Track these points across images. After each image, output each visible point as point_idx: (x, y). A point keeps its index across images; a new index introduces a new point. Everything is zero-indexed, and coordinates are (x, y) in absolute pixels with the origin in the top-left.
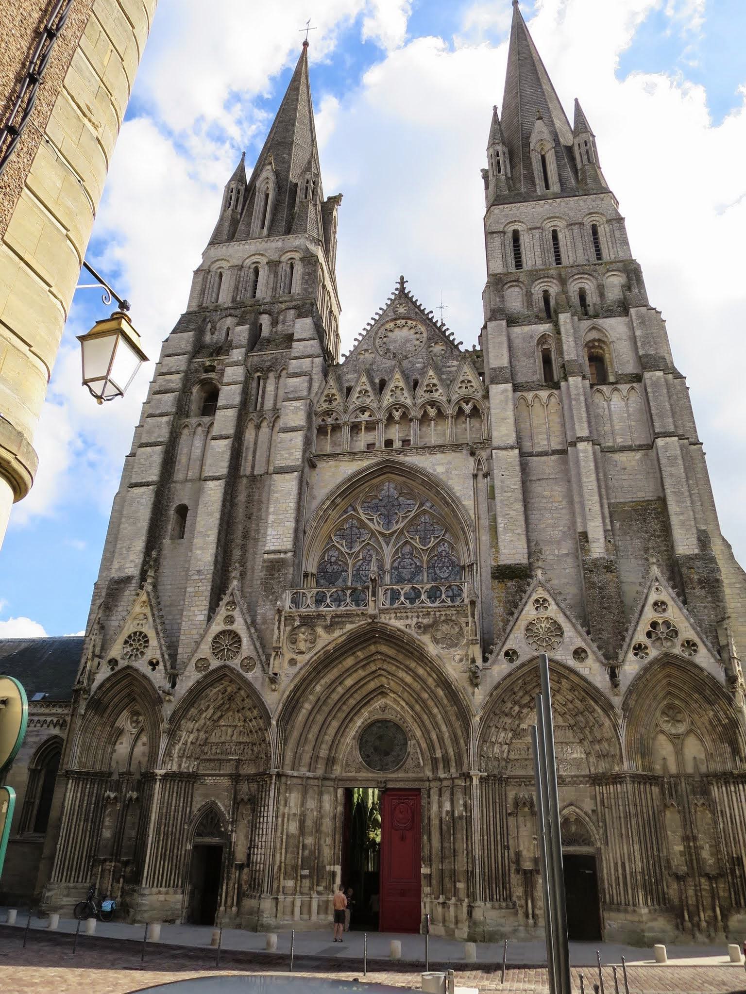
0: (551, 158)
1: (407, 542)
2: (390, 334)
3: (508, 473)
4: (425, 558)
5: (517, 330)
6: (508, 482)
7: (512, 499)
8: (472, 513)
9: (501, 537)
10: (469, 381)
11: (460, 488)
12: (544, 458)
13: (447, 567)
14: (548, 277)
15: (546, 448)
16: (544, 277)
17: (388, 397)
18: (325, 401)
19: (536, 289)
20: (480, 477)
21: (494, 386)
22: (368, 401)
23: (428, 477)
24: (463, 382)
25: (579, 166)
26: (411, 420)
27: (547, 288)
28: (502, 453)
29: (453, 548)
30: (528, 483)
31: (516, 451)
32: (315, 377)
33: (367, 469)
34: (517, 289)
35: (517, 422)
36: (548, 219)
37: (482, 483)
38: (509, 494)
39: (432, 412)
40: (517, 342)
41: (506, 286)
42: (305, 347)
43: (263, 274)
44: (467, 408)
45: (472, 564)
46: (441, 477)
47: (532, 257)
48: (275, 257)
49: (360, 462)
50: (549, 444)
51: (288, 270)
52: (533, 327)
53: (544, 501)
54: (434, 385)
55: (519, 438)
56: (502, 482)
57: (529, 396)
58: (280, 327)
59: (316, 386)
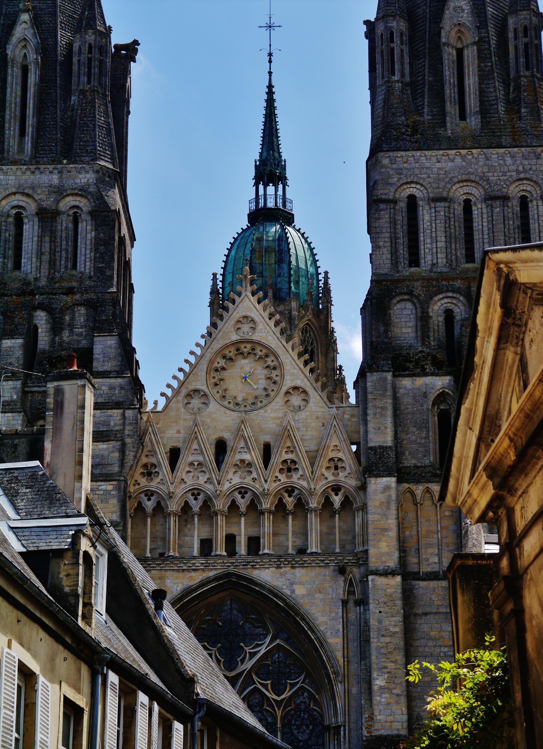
0: (471, 55)
1: (256, 689)
2: (229, 363)
3: (387, 609)
4: (279, 713)
5: (406, 383)
6: (386, 623)
7: (391, 646)
8: (339, 655)
9: (377, 698)
10: (340, 460)
11: (324, 619)
12: (433, 584)
13: (308, 727)
14: (453, 291)
15: (436, 568)
16: (448, 291)
17: (230, 475)
18: (142, 473)
19: (436, 307)
20: (351, 604)
21: (373, 480)
22: (202, 479)
23: (284, 601)
24: (332, 459)
25: (512, 74)
26: (262, 513)
27: (452, 307)
28: (381, 581)
29: (316, 703)
30: (412, 618)
31: (399, 579)
32: (128, 440)
33: (203, 584)
34: (409, 305)
35: (400, 527)
36: (459, 182)
37: (354, 613)
38: (388, 639)
39: (290, 502)
40: (406, 401)
41: (395, 301)
42: (112, 388)
43: (31, 230)
44: (337, 500)
45: (340, 727)
46: (301, 601)
47: (435, 249)
48: (49, 203)
49: (193, 574)
50: (440, 562)
51: (71, 225)
52: (428, 380)
53: (430, 643)
54: (293, 462)
55: (403, 550)
56: (380, 622)
57: (419, 489)
58: (66, 335)
59: (130, 455)
